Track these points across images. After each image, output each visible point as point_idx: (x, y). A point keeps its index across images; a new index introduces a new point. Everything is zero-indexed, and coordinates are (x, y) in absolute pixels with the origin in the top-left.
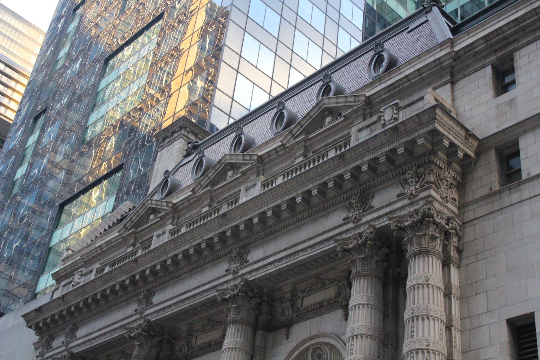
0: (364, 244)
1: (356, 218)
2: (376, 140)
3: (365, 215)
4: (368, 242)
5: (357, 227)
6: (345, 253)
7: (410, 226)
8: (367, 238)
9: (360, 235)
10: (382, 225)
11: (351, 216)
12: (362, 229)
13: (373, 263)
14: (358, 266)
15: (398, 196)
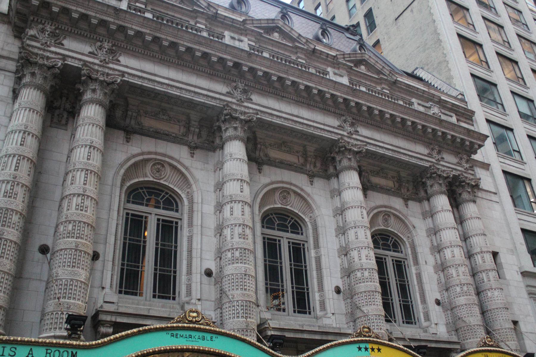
0: (50, 68)
1: (46, 43)
2: (144, 20)
3: (55, 47)
4: (57, 69)
5: (44, 50)
6: (27, 62)
7: (102, 82)
8: (55, 65)
9: (48, 58)
10: (69, 63)
11: (41, 38)
12: (48, 54)
13: (49, 85)
14: (37, 79)
15: (90, 53)
